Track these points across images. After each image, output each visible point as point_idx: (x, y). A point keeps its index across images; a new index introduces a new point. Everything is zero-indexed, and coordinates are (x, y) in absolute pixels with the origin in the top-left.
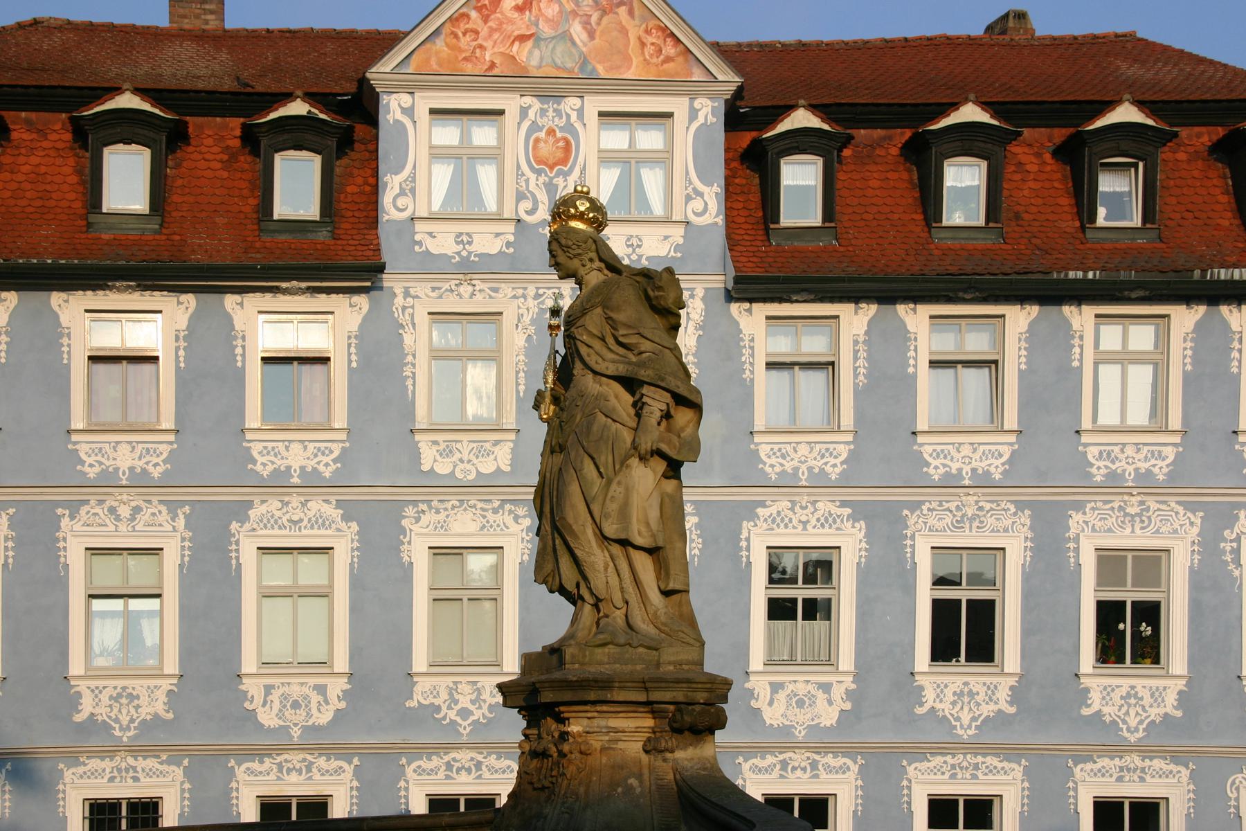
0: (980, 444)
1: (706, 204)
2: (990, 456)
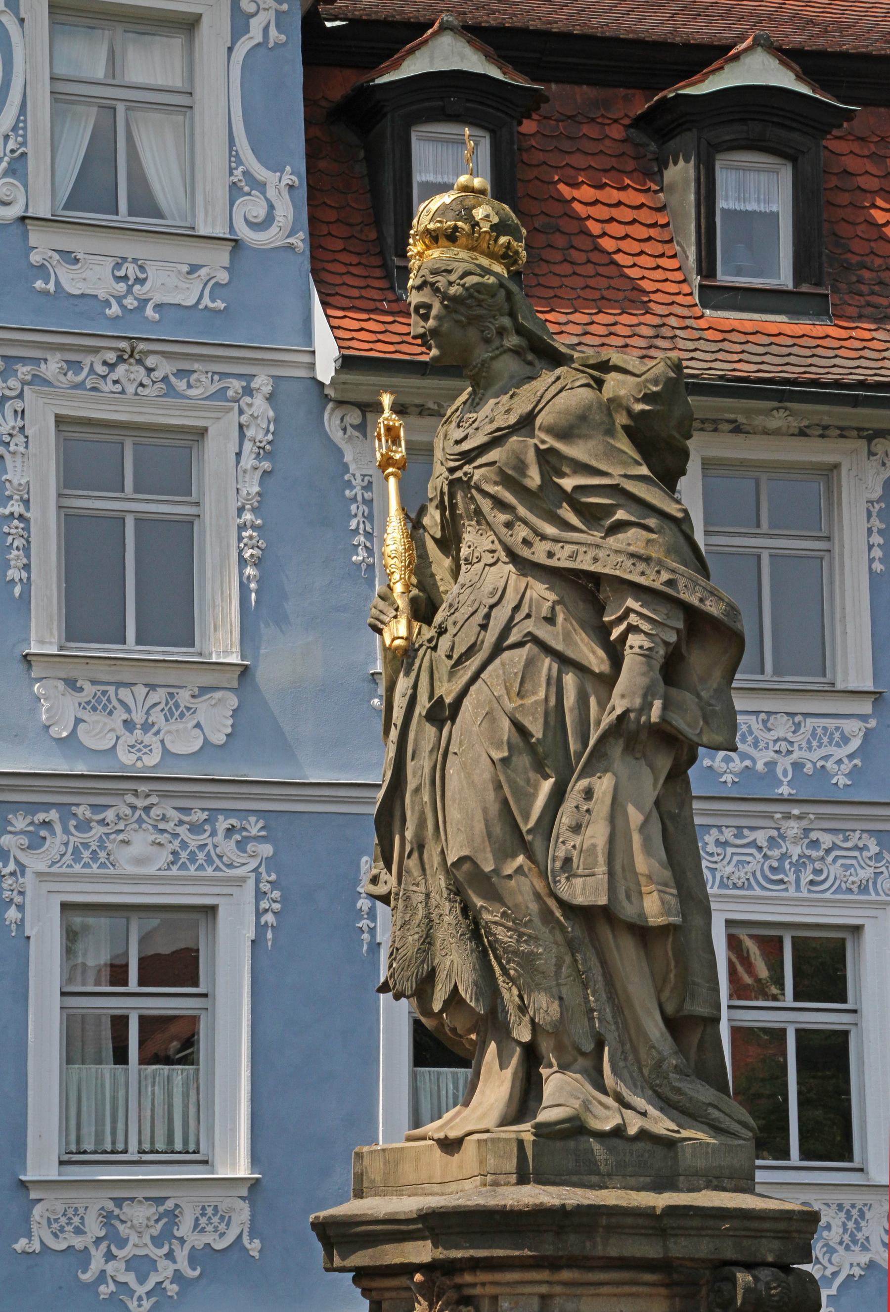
0: (806, 715)
1: (271, 207)
2: (825, 740)
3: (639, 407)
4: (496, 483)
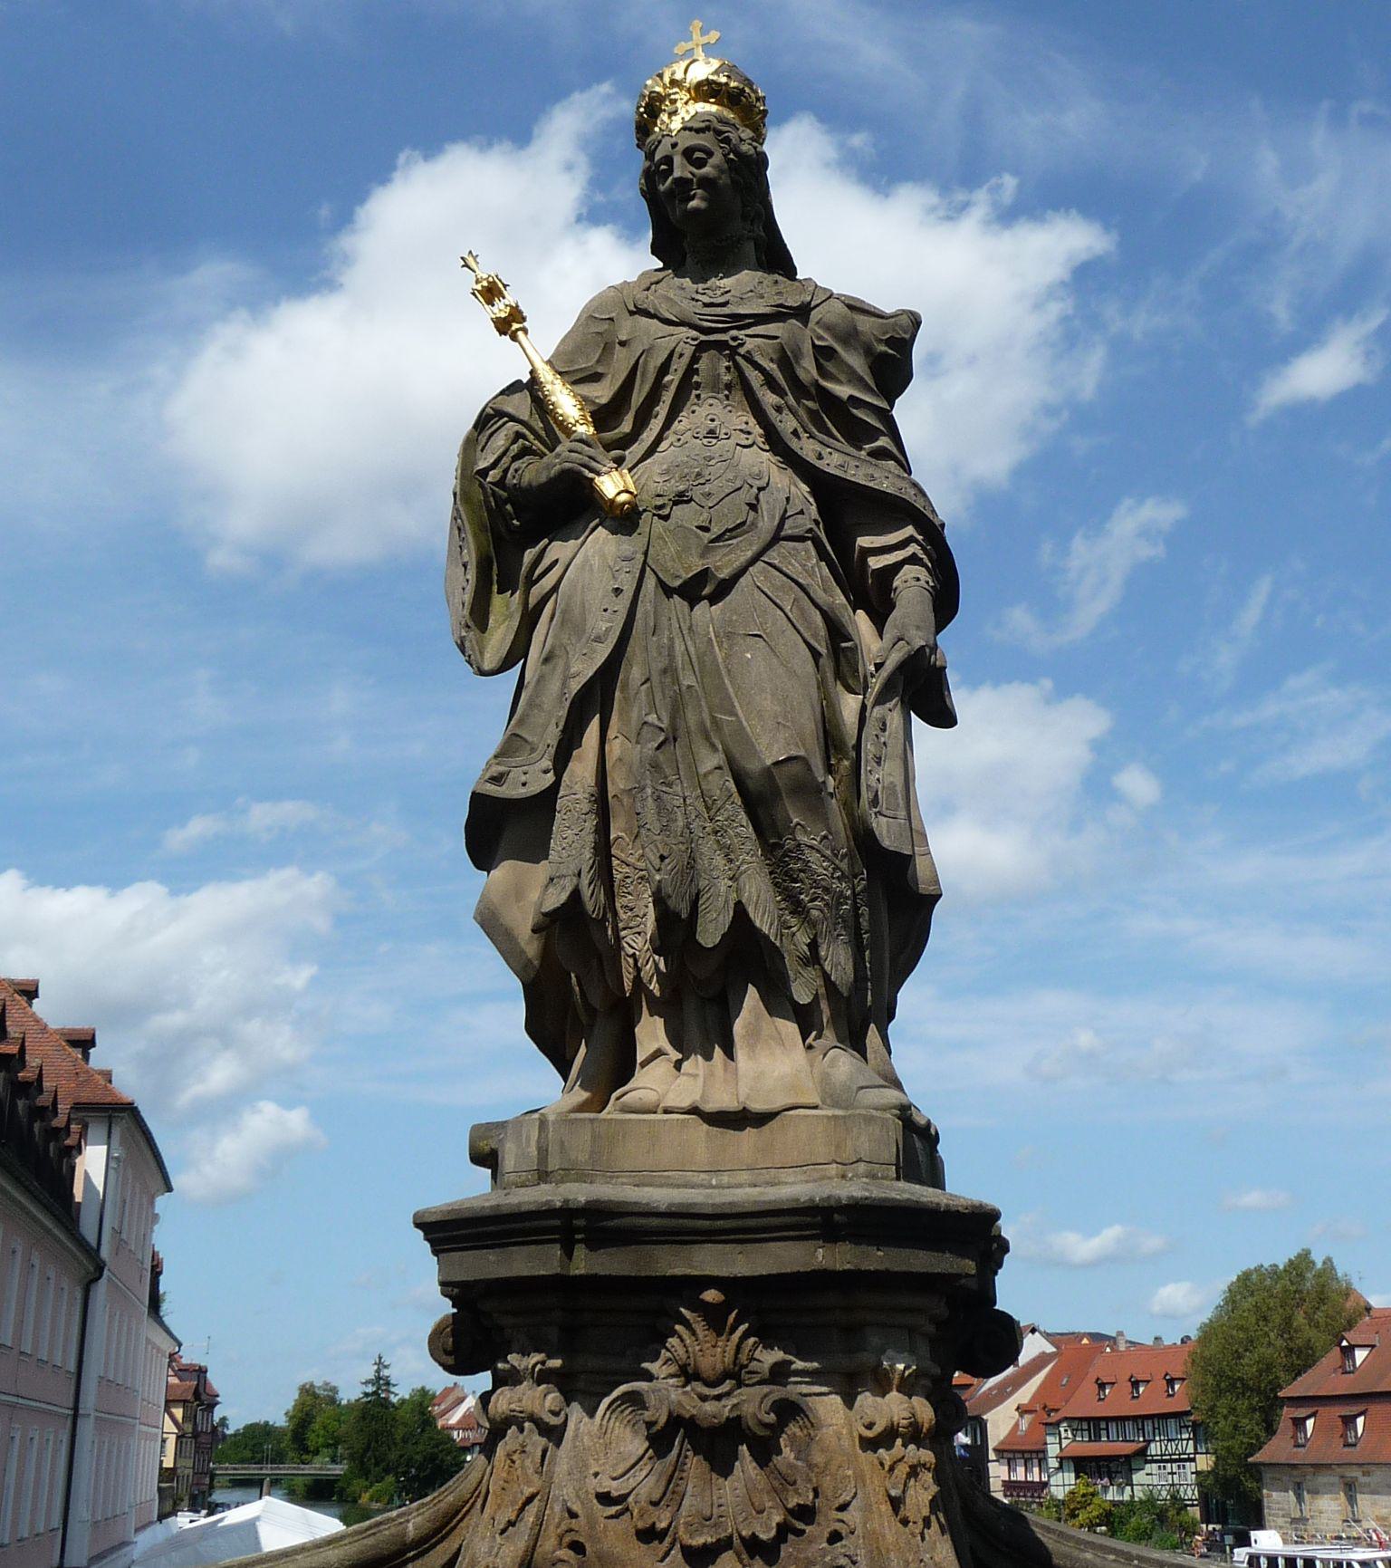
3: (883, 348)
4: (772, 360)
